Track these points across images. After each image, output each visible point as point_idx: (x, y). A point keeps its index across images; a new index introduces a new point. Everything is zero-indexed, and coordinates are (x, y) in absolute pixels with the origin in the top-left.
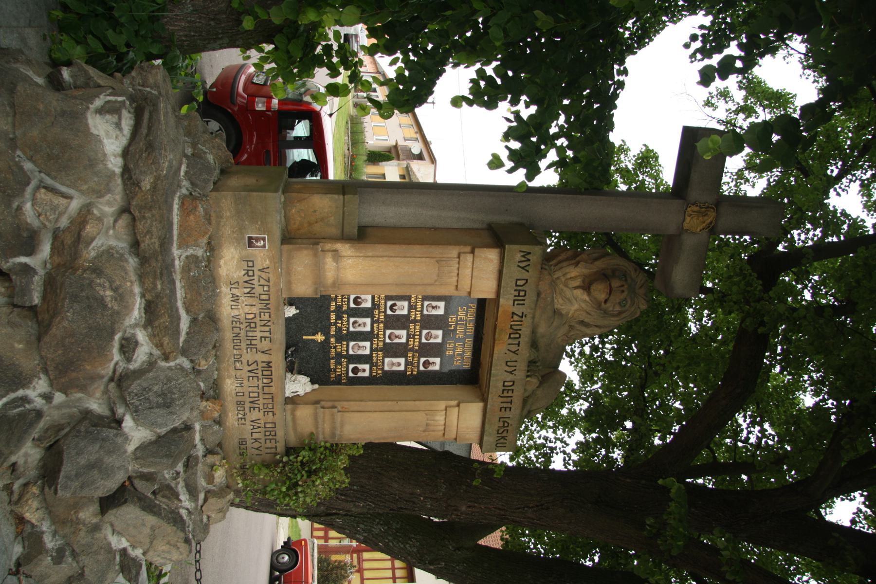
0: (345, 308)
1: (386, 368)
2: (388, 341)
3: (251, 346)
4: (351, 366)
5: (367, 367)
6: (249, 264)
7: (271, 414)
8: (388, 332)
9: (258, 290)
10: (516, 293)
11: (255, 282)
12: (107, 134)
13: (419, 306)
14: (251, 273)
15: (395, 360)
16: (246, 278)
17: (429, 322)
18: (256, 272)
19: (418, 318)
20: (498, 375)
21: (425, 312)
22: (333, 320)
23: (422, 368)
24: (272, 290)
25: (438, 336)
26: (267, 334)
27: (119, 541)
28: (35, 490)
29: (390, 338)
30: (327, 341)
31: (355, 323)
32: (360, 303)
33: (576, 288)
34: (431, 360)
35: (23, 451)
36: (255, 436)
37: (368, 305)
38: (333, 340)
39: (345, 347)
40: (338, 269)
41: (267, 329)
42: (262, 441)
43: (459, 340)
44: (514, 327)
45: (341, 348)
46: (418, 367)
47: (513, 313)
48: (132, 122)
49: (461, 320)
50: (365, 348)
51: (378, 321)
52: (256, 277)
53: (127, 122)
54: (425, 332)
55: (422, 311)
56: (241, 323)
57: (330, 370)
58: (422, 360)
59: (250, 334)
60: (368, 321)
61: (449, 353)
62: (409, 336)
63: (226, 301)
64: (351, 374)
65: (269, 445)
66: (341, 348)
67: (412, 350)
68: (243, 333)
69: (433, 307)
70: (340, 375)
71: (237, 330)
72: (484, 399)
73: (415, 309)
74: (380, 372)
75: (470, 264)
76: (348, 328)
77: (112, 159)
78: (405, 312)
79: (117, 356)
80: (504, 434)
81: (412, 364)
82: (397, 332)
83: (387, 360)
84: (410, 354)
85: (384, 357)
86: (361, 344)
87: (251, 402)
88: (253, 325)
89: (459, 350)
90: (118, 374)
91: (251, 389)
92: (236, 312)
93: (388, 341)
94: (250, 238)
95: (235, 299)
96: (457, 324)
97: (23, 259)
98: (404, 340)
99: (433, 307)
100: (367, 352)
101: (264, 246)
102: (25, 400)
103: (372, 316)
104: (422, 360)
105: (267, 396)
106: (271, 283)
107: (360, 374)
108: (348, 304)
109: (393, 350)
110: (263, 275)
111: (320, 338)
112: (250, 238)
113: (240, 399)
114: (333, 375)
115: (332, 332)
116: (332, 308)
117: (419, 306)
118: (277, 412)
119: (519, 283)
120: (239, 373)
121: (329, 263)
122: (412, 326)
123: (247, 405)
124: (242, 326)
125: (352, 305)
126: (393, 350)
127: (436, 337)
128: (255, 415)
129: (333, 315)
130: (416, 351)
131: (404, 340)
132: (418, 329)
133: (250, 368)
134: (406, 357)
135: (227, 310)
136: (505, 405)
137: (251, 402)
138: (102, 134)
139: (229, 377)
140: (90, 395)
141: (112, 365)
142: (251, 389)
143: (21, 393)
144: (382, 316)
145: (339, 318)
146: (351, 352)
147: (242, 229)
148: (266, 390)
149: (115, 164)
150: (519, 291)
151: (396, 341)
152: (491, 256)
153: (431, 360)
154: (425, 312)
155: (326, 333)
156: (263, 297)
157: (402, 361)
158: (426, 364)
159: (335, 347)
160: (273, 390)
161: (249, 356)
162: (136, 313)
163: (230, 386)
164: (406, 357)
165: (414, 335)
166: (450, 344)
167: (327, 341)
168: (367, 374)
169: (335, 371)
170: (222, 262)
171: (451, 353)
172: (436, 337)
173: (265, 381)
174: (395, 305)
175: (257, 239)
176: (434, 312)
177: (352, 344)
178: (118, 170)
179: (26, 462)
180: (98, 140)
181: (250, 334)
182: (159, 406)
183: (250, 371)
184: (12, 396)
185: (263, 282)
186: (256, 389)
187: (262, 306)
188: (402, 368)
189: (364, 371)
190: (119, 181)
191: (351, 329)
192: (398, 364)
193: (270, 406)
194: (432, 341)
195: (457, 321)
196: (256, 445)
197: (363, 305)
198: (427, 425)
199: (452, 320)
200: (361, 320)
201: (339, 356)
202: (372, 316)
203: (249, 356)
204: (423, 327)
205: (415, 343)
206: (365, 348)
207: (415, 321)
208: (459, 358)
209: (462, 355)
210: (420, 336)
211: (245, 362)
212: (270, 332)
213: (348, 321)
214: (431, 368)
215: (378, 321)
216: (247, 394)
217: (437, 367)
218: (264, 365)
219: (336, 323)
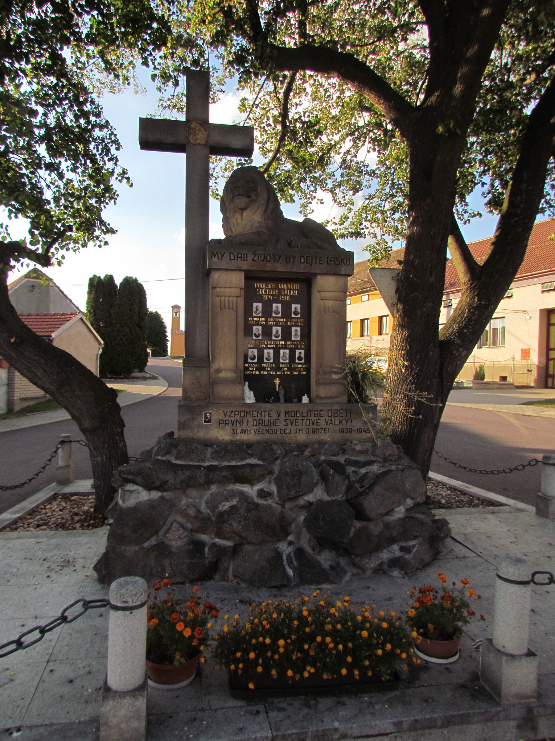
0: (257, 365)
1: (299, 339)
2: (280, 338)
3: (275, 423)
4: (297, 361)
5: (297, 352)
6: (222, 423)
7: (322, 412)
8: (274, 338)
9: (238, 417)
10: (239, 259)
11: (233, 419)
12: (135, 498)
13: (256, 319)
14: (227, 422)
15: (293, 333)
16: (230, 424)
17: (267, 312)
18: (227, 418)
19: (264, 319)
20: (299, 267)
21: (260, 315)
22: (265, 373)
23: (299, 316)
24: (238, 409)
25: (277, 307)
26: (267, 413)
27: (398, 512)
28: (357, 560)
29: (278, 337)
30: (279, 376)
31: (267, 359)
32: (254, 356)
33: (242, 218)
34: (293, 310)
35: (322, 562)
36: (337, 423)
37: (255, 351)
38: (279, 373)
39: (284, 366)
40: (226, 370)
41: (263, 413)
42: (341, 419)
43: (279, 292)
44: (262, 258)
45: (285, 368)
46: (298, 318)
47: (253, 260)
48: (131, 484)
49: (266, 292)
50: (284, 353)
51: (267, 345)
52: (230, 419)
53: (130, 487)
54: (274, 315)
55: (260, 317)
56: (259, 428)
57: (300, 374)
58: (293, 316)
59: (266, 424)
60: (266, 351)
61: (288, 298)
62: (277, 325)
63: (244, 437)
64: (303, 361)
65: (344, 414)
66: (285, 368)
67: (286, 323)
68: (266, 428)
69: (257, 310)
70: (304, 368)
71: (264, 431)
72: (316, 275)
73: (258, 321)
74: (301, 343)
75: (222, 289)
76: (271, 363)
77: (151, 497)
78: (260, 328)
79: (270, 501)
80: (340, 260)
81: (296, 322)
82: (274, 332)
83: (293, 338)
84: (289, 324)
85: (291, 341)
86: (281, 355)
87: (313, 424)
88: (261, 422)
89: (287, 292)
90: (279, 502)
91: (304, 424)
92: (252, 431)
93: (280, 338)
94: (205, 422)
95: (243, 431)
96: (269, 295)
97: (206, 550)
98: (279, 328)
99: (257, 310)
100: (287, 351)
101: (210, 414)
102: (289, 556)
103: (263, 349)
104: (293, 316)
105: (309, 415)
106: (234, 410)
107: (303, 356)
108: (255, 363)
109: (286, 334)
110: (228, 414)
111: (277, 381)
112: (205, 422)
113: (311, 431)
114: (304, 373)
115: (274, 373)
116: (258, 373)
117: (256, 319)
118: (320, 408)
119: (232, 258)
120: (293, 431)
121: (223, 375)
122: (270, 323)
123: (315, 427)
124: (262, 428)
125: (256, 361)
126: (286, 334)
127: (277, 307)
128: (322, 422)
129: (262, 373)
130: (287, 320)
131: (279, 328)
132: (272, 319)
133: (290, 424)
134: (291, 326)
135: (251, 437)
136: (318, 261)
137: (313, 424)
138: (136, 501)
139: (296, 437)
140: (295, 519)
141: (274, 505)
142: (304, 424)
143: (285, 558)
144: (263, 342)
145: (263, 369)
146: (287, 361)
147: (199, 426)
148: (305, 414)
149: (155, 495)
150: (238, 257)
151: (280, 333)
152: (215, 276)
153: (293, 310)
154: (260, 315)
155: (275, 377)
156: (242, 415)
157: (293, 329)
158: (296, 313)
159: (284, 371)
160: (305, 411)
161: (281, 425)
162: (246, 488)
163: (302, 437)
164: (291, 326)
165: (276, 321)
166: (282, 298)
167: (279, 376)
168: (303, 352)
169: (300, 371)
170: (221, 438)
171: (288, 297)
172: (277, 307)
173: (298, 415)
174: (255, 334)
175: (206, 417)
176: (260, 309)
177: (281, 361)
178: (159, 494)
179: (329, 560)
180: (139, 503)
181: (266, 424)
182: (300, 479)
183: (292, 424)
184: (285, 562)
185: (233, 415)
186: (304, 421)
187: (248, 415)
188: (299, 329)
189: (300, 353)
190: (165, 494)
191: (272, 361)
192: (296, 333)
193: (316, 413)
194: (280, 310)
195: (266, 294)
196: (344, 422)
197: (256, 354)
198: (333, 312)
199: (266, 298)
200: (266, 356)
201: (290, 369)
202: (263, 349)
203: (281, 425)
204: (271, 316)
205: (282, 321)
206: (284, 353)
207: (266, 321)
208: (292, 292)
209: (290, 290)
210: (276, 318)
211: (285, 427)
212: (265, 411)
213: (266, 363)
214: (299, 310)
215: (267, 345)
216: (307, 427)
217: (299, 306)
218: (287, 415)
219: (268, 371)
